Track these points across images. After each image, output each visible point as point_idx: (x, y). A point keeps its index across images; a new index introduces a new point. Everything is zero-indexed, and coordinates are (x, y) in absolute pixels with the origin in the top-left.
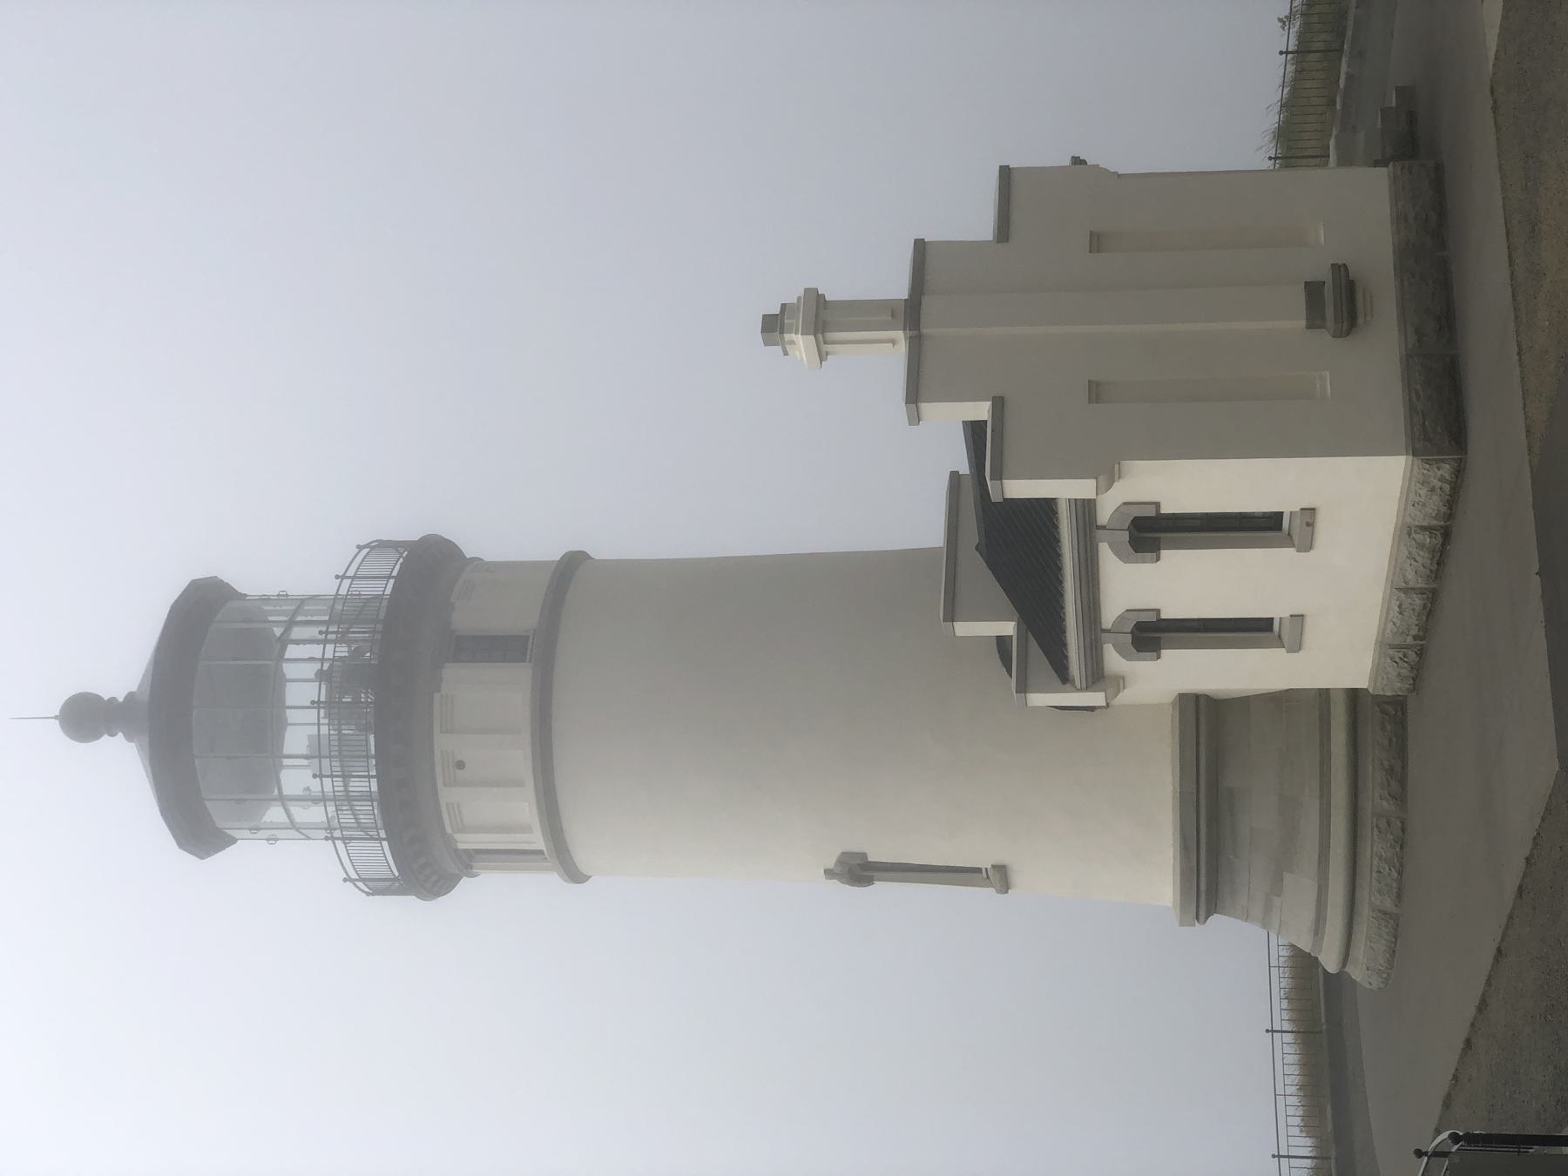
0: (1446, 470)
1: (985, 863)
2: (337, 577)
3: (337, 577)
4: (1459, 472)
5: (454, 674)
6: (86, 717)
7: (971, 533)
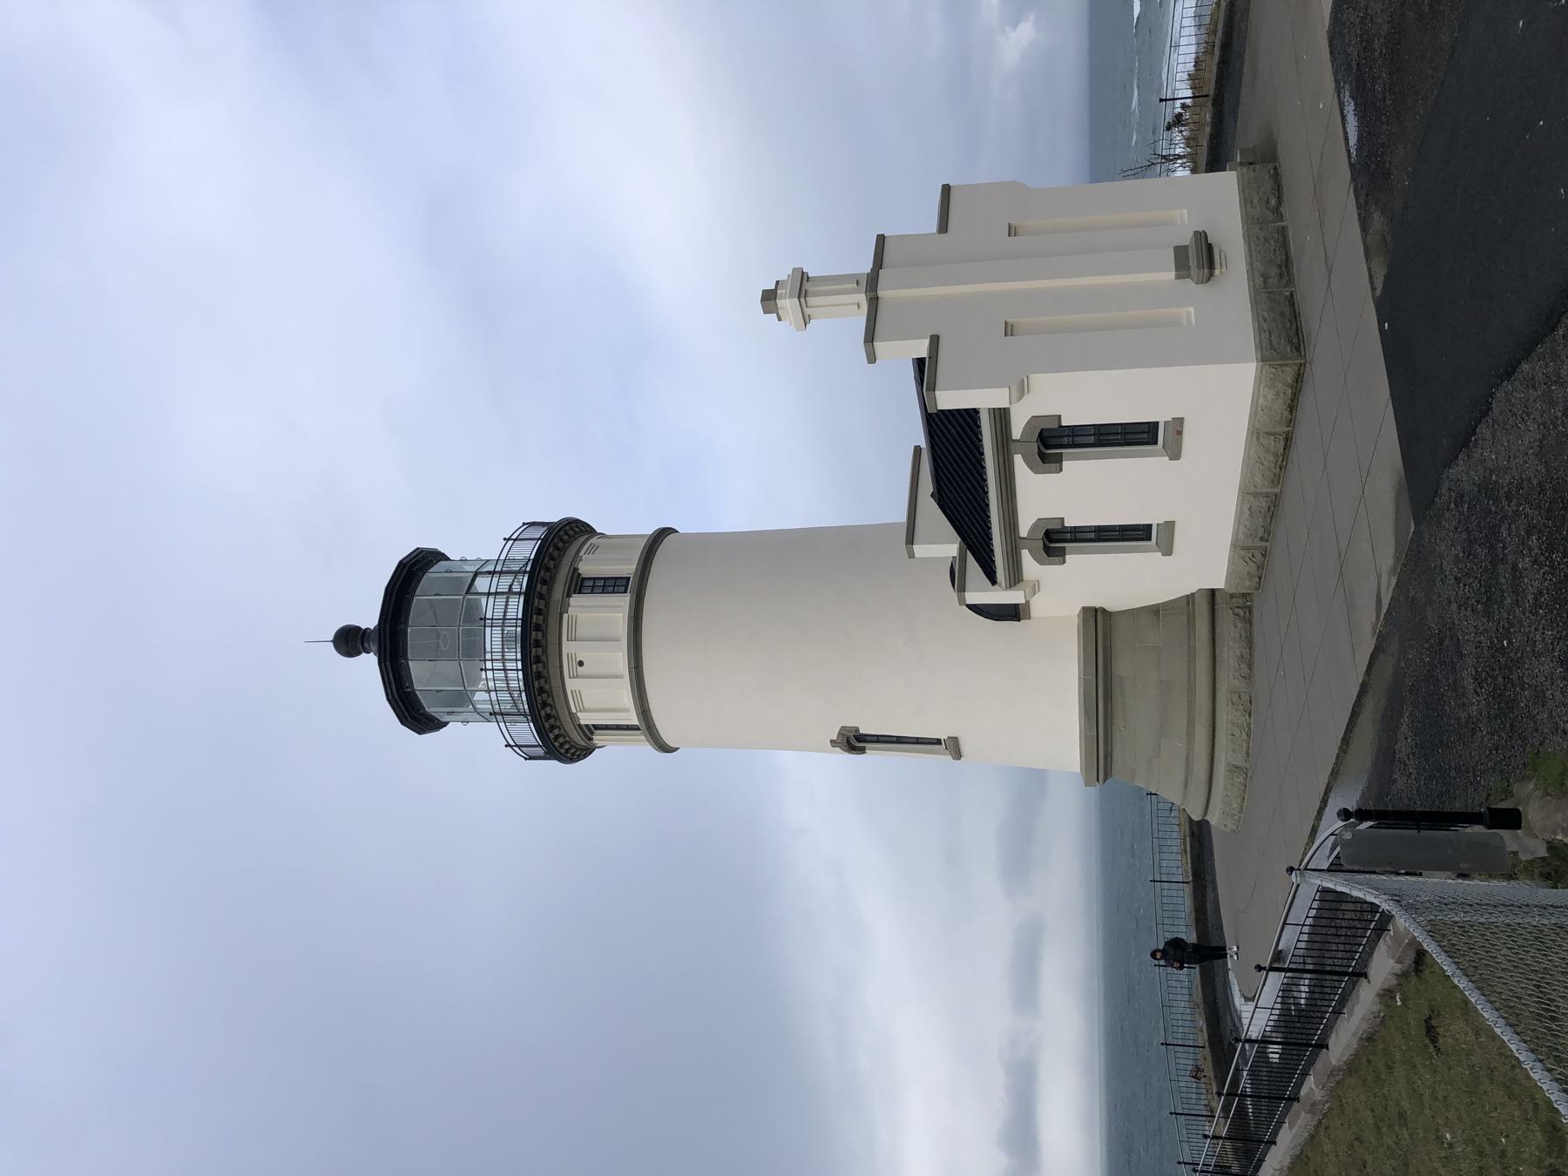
0: (1289, 375)
1: (942, 737)
4: (1299, 378)
6: (349, 641)
7: (927, 484)
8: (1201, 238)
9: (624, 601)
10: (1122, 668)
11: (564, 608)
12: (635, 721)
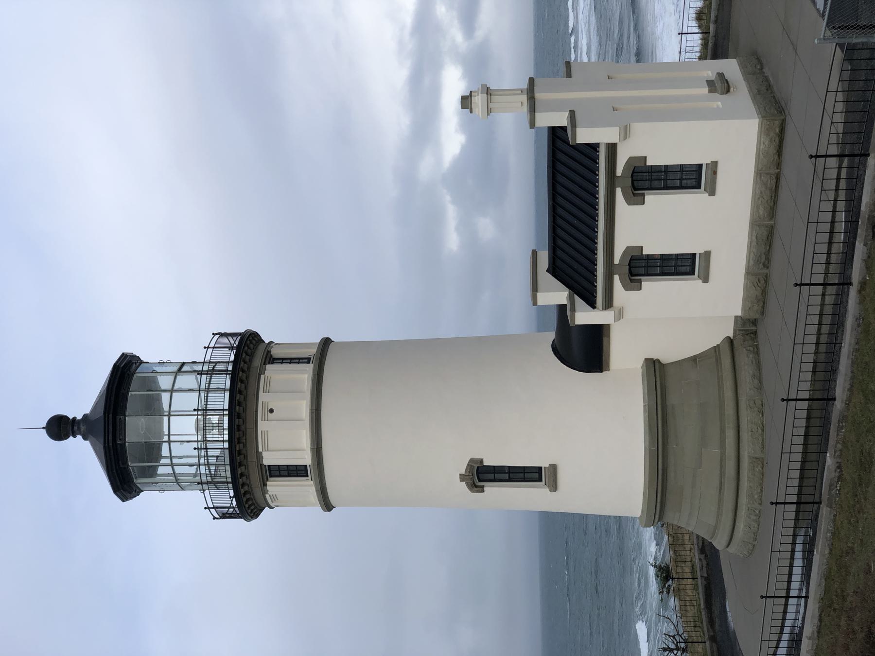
1: (544, 464)
5: (271, 370)
6: (60, 428)
8: (721, 75)
9: (310, 368)
10: (673, 399)
11: (262, 371)
12: (305, 459)
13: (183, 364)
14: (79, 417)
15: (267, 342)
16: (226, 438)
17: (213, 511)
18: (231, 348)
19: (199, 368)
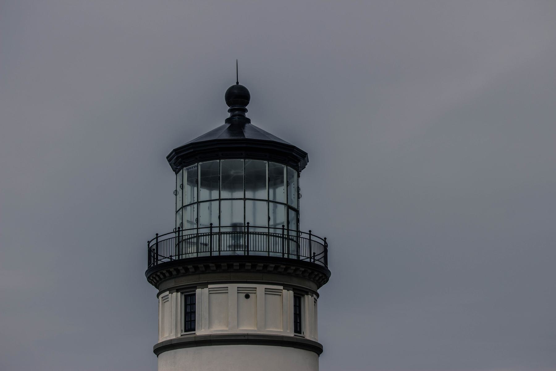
2: (325, 239)
3: (325, 239)
5: (289, 295)
6: (238, 98)
9: (290, 333)
11: (287, 287)
13: (297, 211)
14: (247, 115)
15: (318, 291)
16: (222, 254)
17: (154, 242)
18: (313, 256)
19: (293, 226)
